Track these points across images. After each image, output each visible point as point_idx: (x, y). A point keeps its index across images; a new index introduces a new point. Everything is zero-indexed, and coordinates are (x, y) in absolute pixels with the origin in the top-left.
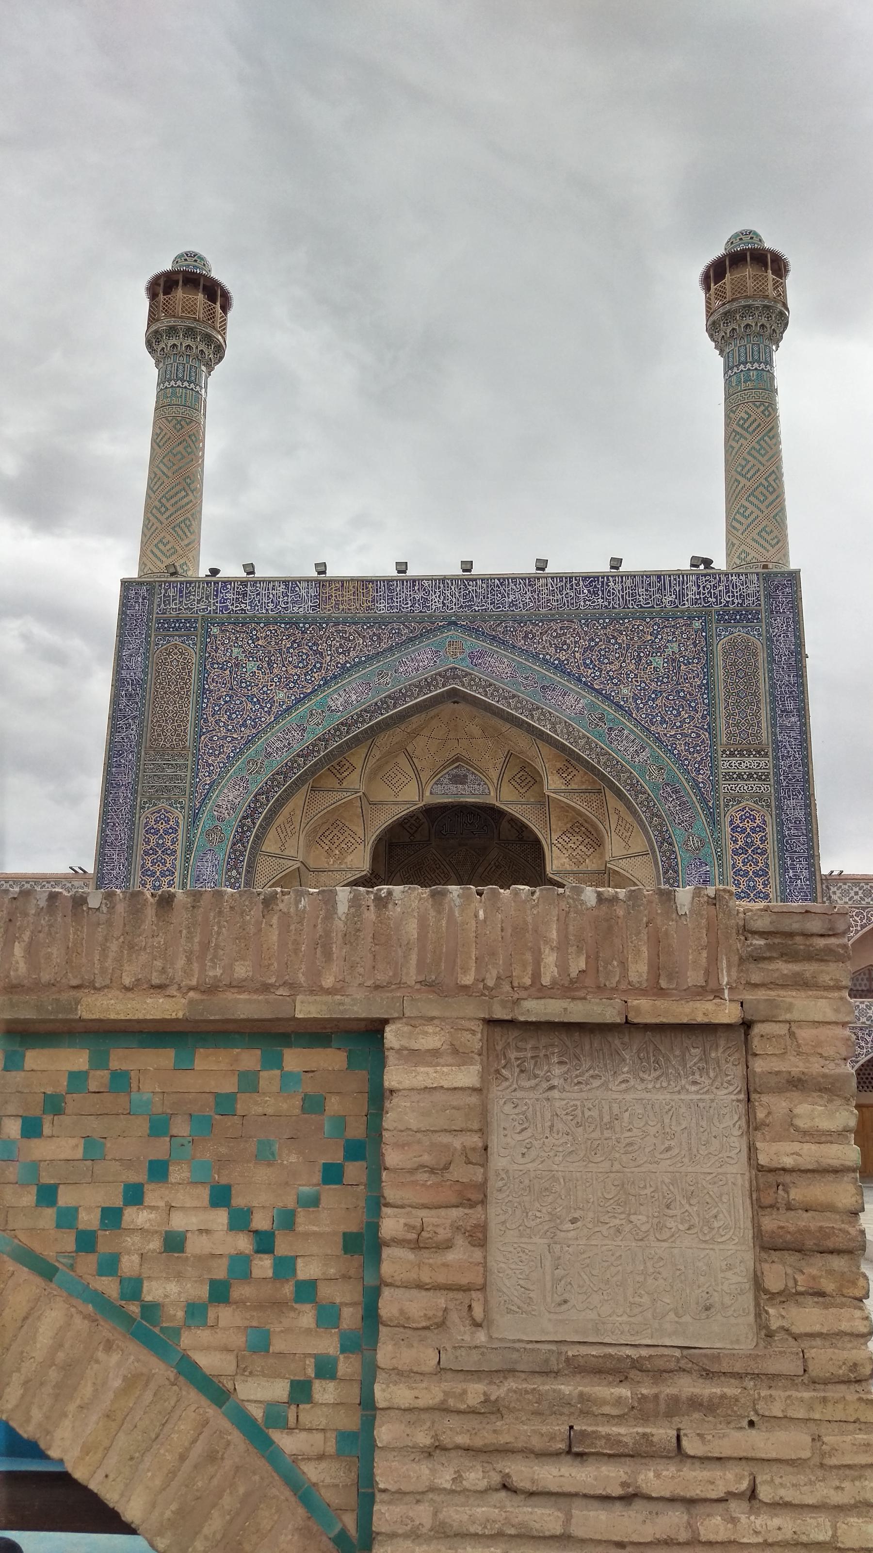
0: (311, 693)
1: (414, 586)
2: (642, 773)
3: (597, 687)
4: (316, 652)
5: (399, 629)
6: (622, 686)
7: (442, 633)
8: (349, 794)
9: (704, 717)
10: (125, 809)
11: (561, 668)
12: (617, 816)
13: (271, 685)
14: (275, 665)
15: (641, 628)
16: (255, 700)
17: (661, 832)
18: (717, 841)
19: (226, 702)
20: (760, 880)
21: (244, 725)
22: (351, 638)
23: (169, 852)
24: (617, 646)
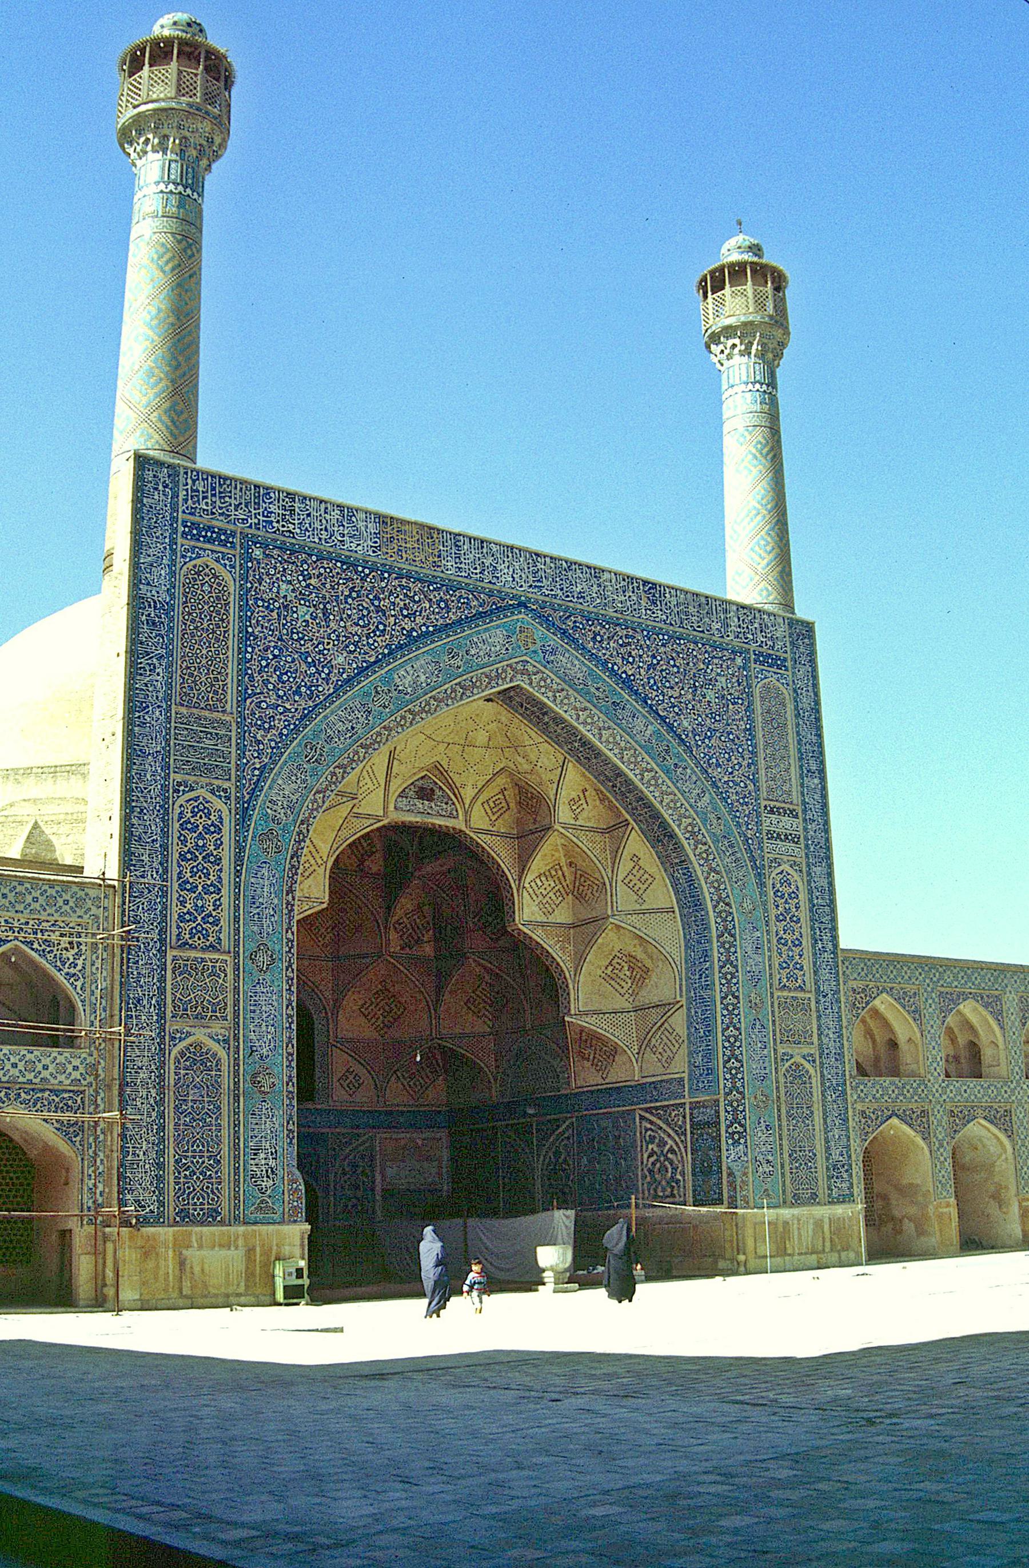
0: (375, 662)
1: (482, 547)
2: (704, 821)
3: (661, 713)
4: (378, 610)
5: (468, 599)
6: (682, 717)
7: (513, 613)
8: (345, 799)
9: (749, 765)
10: (155, 789)
11: (627, 683)
12: (633, 864)
13: (329, 643)
14: (332, 617)
15: (695, 653)
16: (310, 660)
17: (717, 889)
18: (764, 904)
19: (275, 657)
20: (797, 950)
21: (297, 692)
22: (417, 598)
23: (212, 859)
24: (675, 669)
